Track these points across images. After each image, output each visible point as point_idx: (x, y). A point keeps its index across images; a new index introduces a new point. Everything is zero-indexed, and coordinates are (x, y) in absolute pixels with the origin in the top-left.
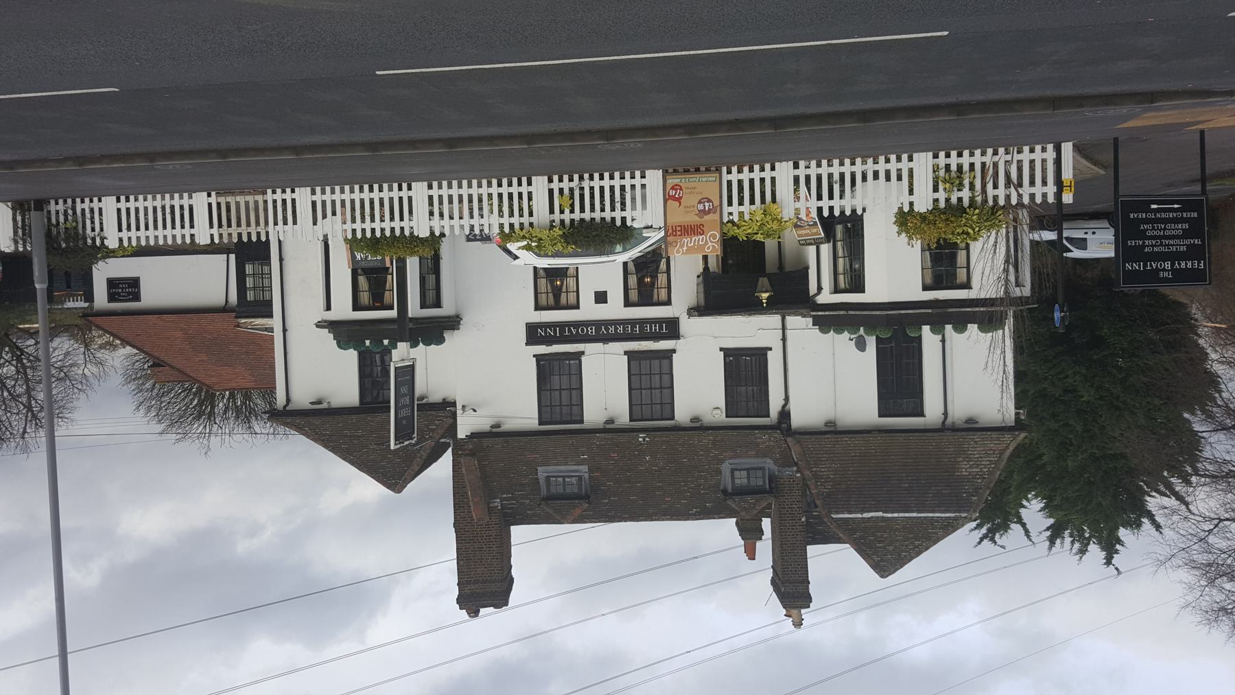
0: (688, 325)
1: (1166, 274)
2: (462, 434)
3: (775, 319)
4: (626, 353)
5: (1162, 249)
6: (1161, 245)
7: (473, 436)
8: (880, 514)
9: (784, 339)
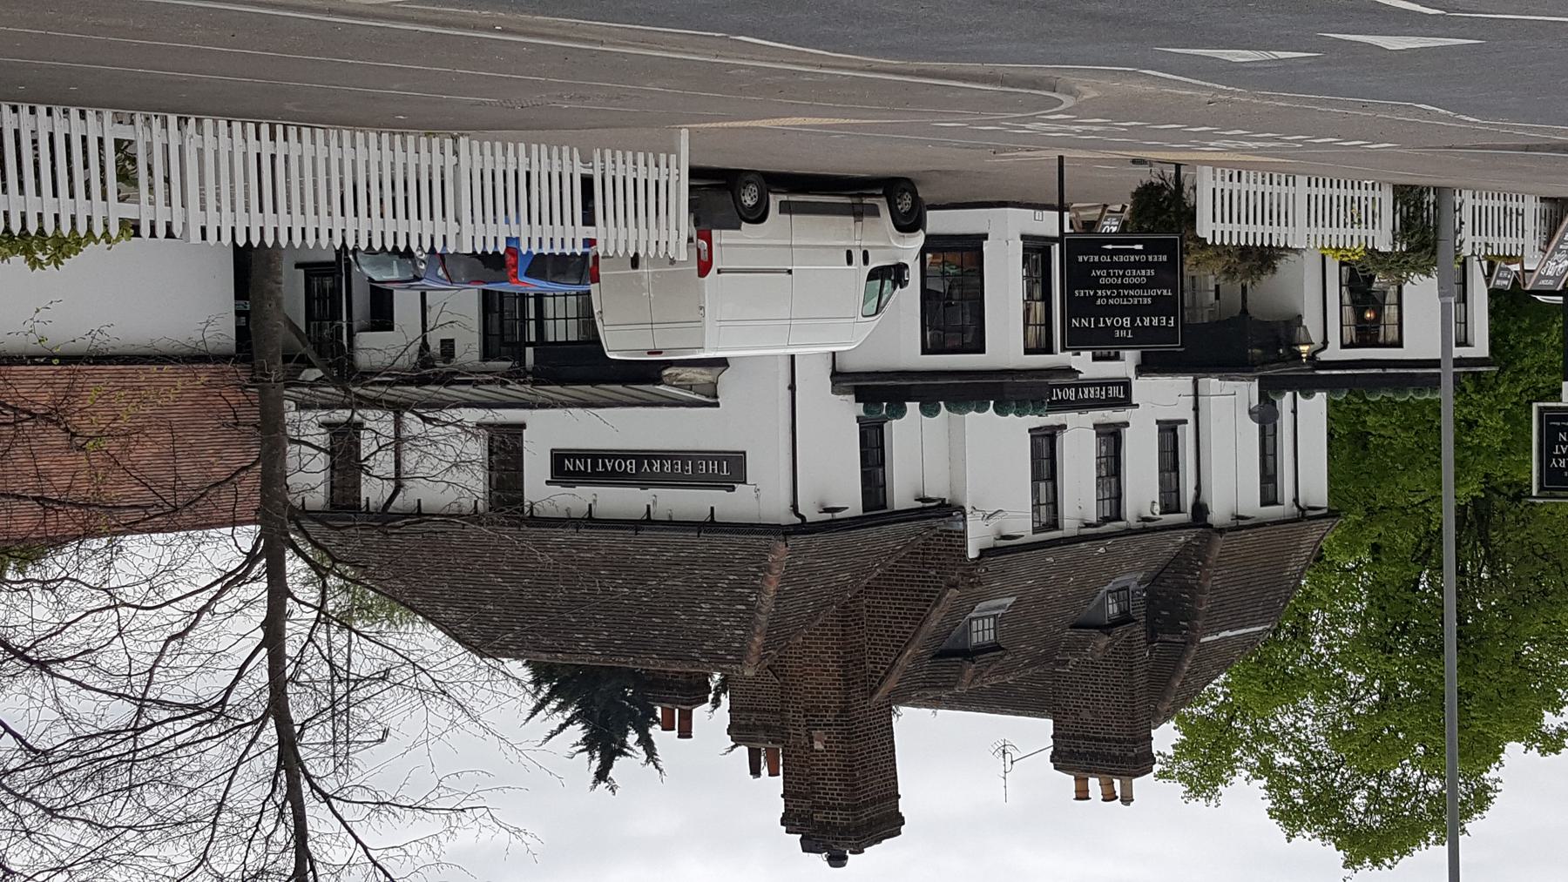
0: (1144, 388)
1: (1123, 333)
2: (972, 553)
3: (1184, 382)
4: (1096, 426)
5: (1119, 301)
6: (1118, 295)
7: (984, 553)
9: (1196, 409)
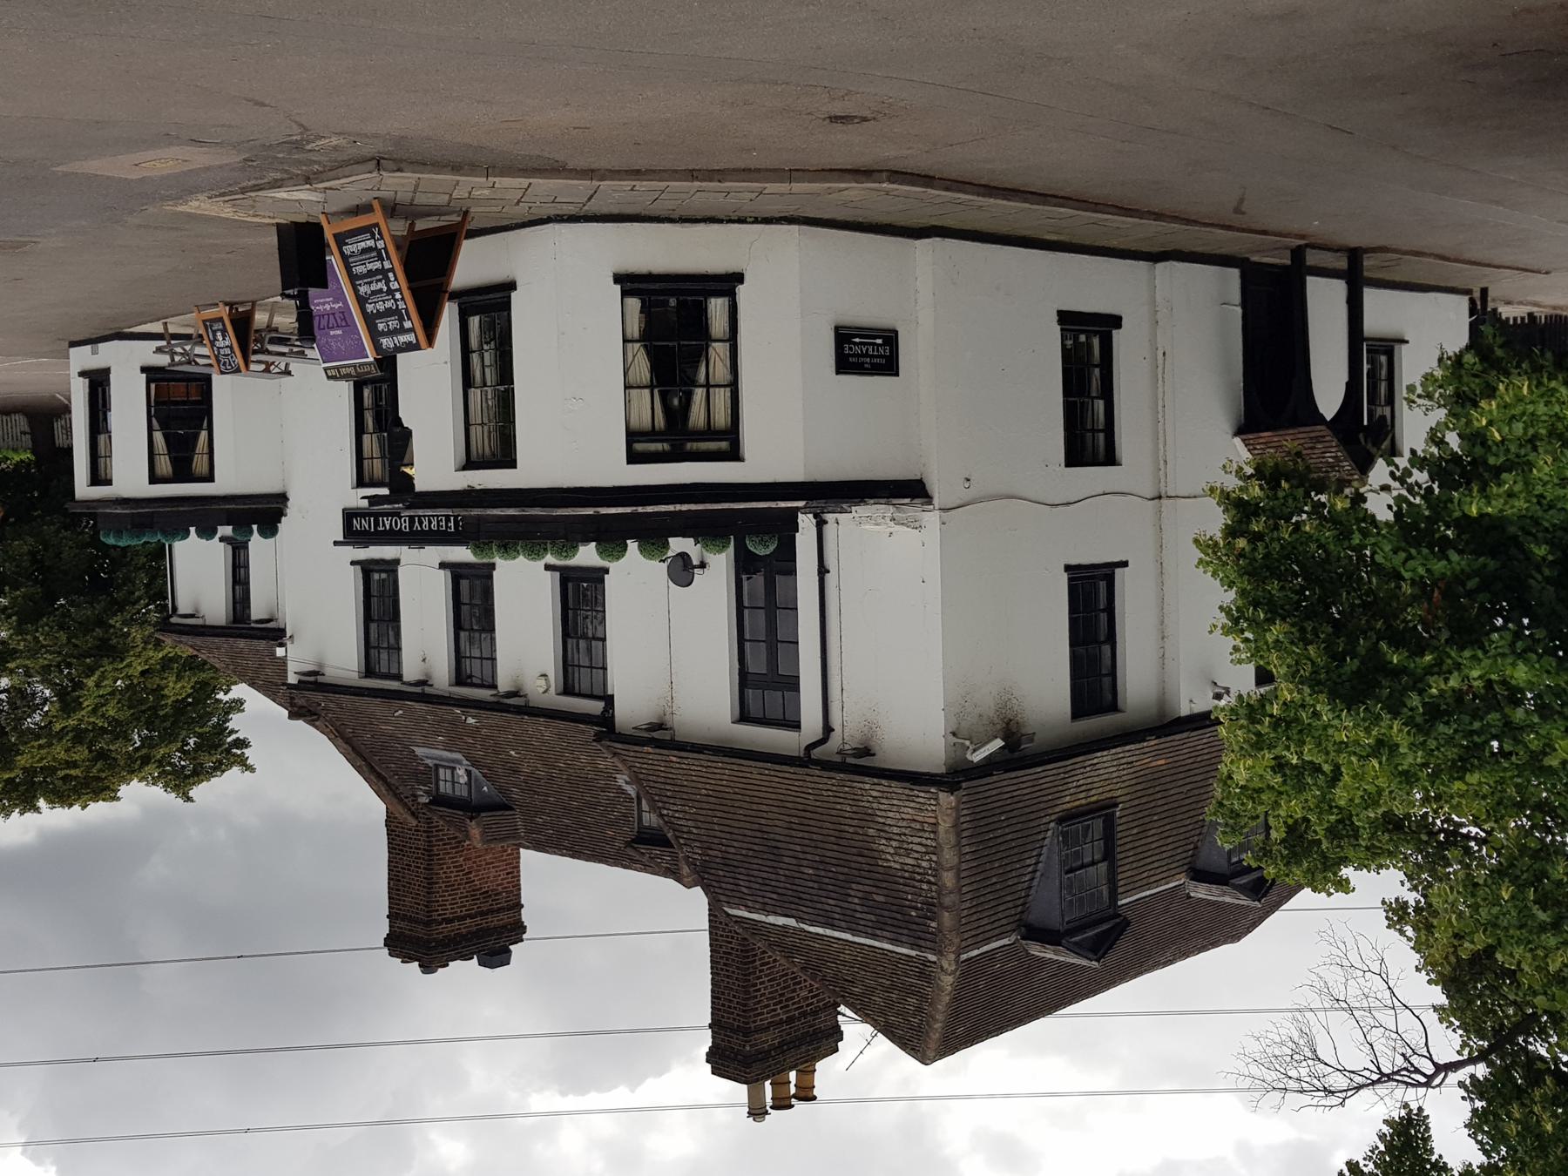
8: (792, 922)
